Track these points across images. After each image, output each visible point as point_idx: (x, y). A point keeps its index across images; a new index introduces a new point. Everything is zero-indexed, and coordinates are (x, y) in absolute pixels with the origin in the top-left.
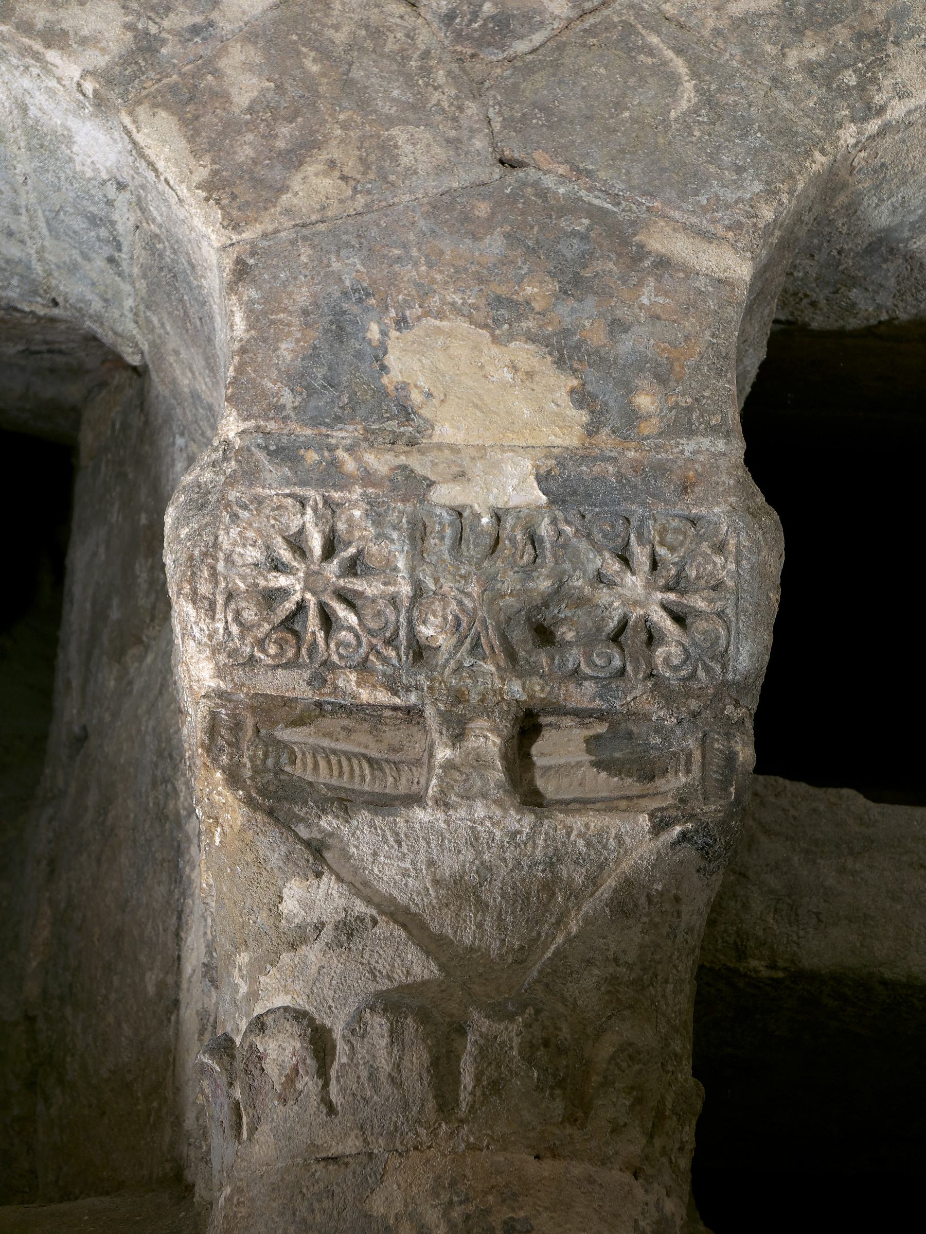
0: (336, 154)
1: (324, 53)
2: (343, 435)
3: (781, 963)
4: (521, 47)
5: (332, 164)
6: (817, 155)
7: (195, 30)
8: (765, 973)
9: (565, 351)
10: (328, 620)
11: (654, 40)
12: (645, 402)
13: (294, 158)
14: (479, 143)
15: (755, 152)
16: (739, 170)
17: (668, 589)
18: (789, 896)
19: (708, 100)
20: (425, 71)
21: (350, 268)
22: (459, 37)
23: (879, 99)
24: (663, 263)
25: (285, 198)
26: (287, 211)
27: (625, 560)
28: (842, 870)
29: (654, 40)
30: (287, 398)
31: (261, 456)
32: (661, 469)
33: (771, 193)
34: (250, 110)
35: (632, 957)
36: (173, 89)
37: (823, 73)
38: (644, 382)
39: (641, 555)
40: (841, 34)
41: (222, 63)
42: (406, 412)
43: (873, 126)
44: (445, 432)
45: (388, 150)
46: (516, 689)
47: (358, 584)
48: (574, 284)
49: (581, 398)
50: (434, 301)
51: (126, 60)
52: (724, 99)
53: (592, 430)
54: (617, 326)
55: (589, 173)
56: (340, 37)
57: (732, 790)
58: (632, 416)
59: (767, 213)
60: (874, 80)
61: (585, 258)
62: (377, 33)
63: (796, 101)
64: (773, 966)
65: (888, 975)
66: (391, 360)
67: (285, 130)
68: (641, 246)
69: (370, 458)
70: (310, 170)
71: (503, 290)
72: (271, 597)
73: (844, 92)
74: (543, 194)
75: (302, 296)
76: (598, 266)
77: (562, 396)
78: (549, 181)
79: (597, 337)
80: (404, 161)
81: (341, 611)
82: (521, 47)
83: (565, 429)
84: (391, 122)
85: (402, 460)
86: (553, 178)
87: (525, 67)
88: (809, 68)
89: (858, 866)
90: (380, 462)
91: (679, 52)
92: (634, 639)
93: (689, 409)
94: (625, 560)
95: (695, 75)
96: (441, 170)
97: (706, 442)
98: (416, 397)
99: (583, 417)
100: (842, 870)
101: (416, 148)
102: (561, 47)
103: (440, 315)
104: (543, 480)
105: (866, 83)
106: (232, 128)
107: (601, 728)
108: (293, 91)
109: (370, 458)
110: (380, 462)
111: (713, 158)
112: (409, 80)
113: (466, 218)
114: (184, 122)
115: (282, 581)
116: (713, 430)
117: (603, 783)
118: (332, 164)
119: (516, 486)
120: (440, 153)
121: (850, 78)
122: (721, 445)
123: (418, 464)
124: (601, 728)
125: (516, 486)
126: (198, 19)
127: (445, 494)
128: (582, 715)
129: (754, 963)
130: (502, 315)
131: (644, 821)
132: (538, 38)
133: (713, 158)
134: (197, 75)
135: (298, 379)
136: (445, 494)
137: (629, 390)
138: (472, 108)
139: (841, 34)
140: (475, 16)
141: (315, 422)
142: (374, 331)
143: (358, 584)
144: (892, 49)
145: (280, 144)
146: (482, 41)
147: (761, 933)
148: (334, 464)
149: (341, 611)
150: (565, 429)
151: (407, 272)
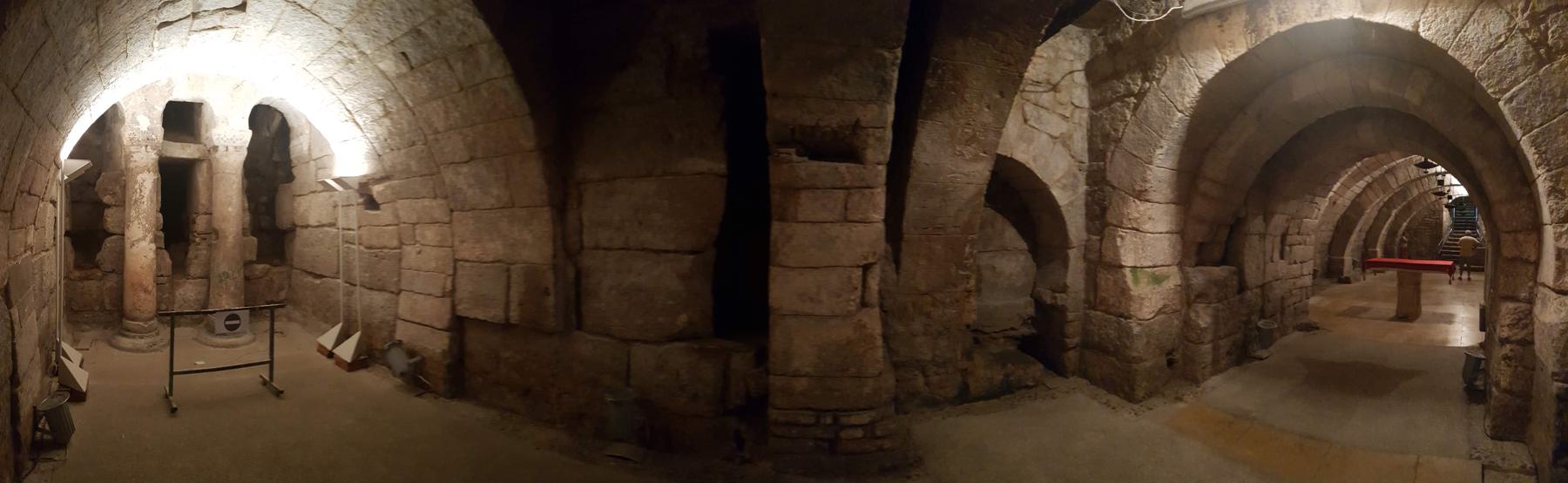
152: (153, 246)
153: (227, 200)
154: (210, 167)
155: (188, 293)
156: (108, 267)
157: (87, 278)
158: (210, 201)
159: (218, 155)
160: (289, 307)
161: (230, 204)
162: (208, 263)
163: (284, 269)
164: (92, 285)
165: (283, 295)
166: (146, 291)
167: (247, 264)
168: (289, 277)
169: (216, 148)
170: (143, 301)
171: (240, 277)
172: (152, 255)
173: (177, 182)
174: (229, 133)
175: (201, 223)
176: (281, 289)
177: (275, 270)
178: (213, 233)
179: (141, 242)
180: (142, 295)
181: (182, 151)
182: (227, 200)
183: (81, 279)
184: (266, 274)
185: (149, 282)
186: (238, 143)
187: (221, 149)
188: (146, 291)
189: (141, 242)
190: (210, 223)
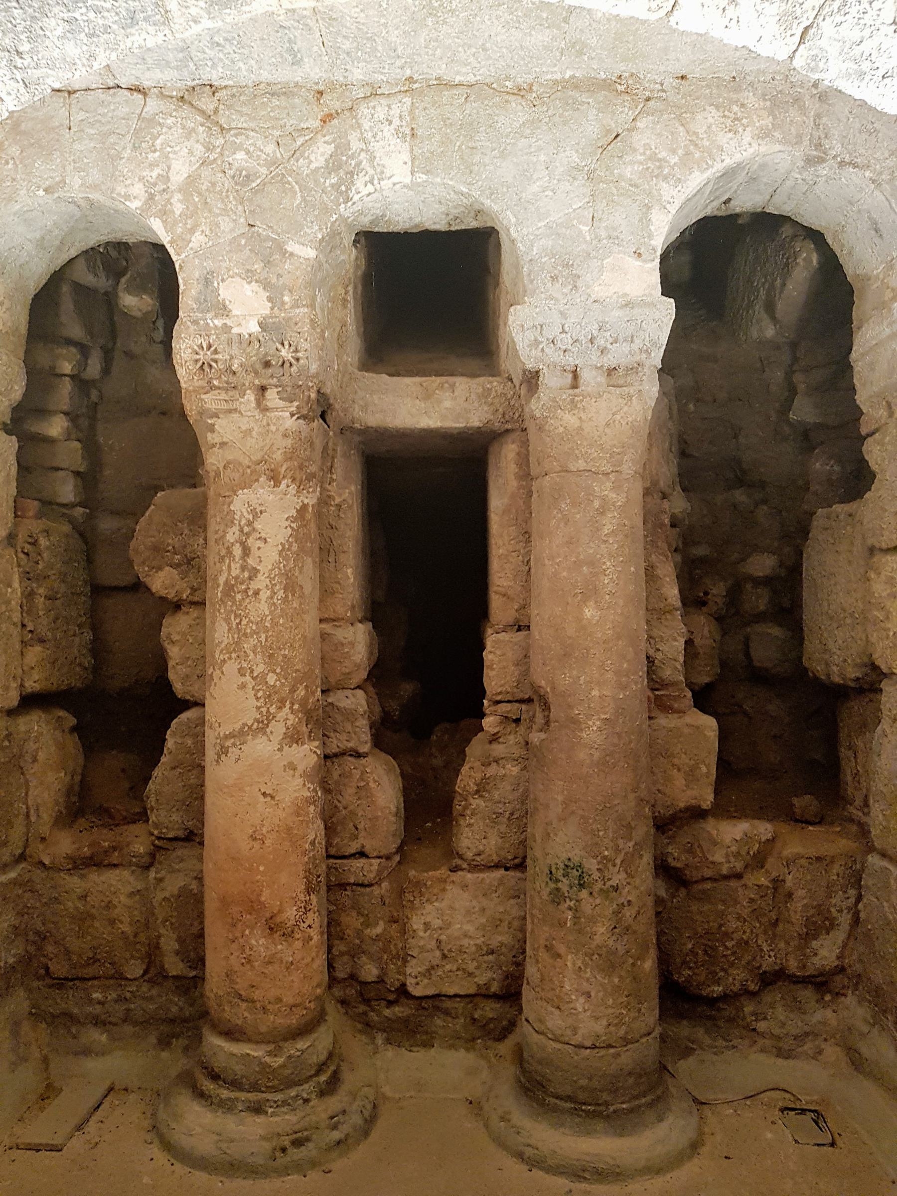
0: (204, 228)
1: (200, 194)
2: (209, 316)
4: (254, 185)
5: (203, 231)
7: (164, 190)
9: (266, 285)
10: (211, 366)
11: (290, 179)
12: (286, 299)
13: (192, 231)
14: (242, 220)
15: (316, 216)
16: (312, 222)
17: (294, 352)
19: (304, 199)
20: (227, 197)
21: (209, 264)
22: (236, 184)
23: (351, 196)
24: (292, 254)
25: (190, 245)
26: (191, 249)
27: (283, 344)
29: (290, 179)
30: (194, 306)
31: (189, 323)
32: (290, 318)
33: (321, 229)
34: (180, 216)
35: (289, 446)
36: (160, 210)
37: (336, 187)
38: (286, 292)
39: (286, 343)
40: (342, 173)
41: (172, 201)
42: (225, 307)
43: (350, 204)
44: (235, 312)
45: (218, 225)
46: (257, 382)
47: (216, 356)
48: (268, 263)
49: (270, 299)
50: (231, 273)
51: (146, 203)
52: (308, 198)
53: (272, 309)
54: (279, 276)
55: (271, 227)
56: (204, 187)
58: (283, 303)
60: (350, 189)
61: (271, 255)
62: (213, 184)
63: (329, 198)
66: (220, 292)
67: (189, 222)
69: (216, 322)
70: (196, 234)
71: (249, 267)
72: (197, 361)
73: (341, 193)
74: (259, 235)
75: (197, 274)
76: (274, 257)
77: (265, 299)
78: (260, 230)
79: (274, 280)
80: (222, 228)
81: (214, 364)
82: (254, 185)
83: (265, 309)
84: (218, 215)
85: (225, 321)
86: (261, 229)
87: (256, 191)
88: (332, 186)
90: (218, 322)
91: (296, 183)
92: (287, 365)
94: (283, 344)
95: (301, 191)
96: (232, 230)
97: (302, 310)
98: (227, 303)
99: (270, 305)
101: (225, 224)
102: (264, 185)
103: (233, 277)
104: (260, 324)
105: (348, 189)
106: (175, 223)
107: (280, 389)
108: (191, 208)
109: (216, 322)
110: (218, 322)
111: (305, 219)
112: (223, 202)
113: (239, 245)
114: (163, 222)
115: (198, 357)
116: (303, 306)
117: (282, 403)
118: (203, 231)
119: (253, 327)
120: (232, 225)
121: (343, 188)
123: (229, 322)
124: (280, 389)
125: (253, 327)
126: (165, 186)
127: (235, 330)
128: (276, 386)
130: (249, 276)
131: (288, 414)
132: (258, 181)
134: (166, 206)
135: (197, 300)
136: (235, 330)
137: (283, 295)
138: (240, 208)
139: (342, 173)
140: (240, 175)
141: (202, 312)
142: (216, 284)
143: (216, 356)
144: (355, 177)
145: (189, 226)
146: (243, 186)
148: (207, 324)
149: (214, 364)
150: (265, 309)
151: (224, 265)
152: (306, 755)
153: (583, 589)
154: (524, 460)
155: (451, 922)
156: (167, 818)
157: (94, 862)
158: (527, 575)
159: (536, 406)
160: (853, 1010)
161: (590, 592)
162: (521, 816)
163: (832, 843)
164: (116, 885)
165: (826, 952)
166: (273, 927)
167: (667, 824)
168: (856, 879)
169: (532, 379)
170: (267, 966)
171: (640, 885)
172: (296, 789)
173: (425, 540)
174: (591, 315)
175: (499, 658)
176: (819, 924)
177: (797, 844)
178: (532, 700)
179: (260, 750)
180: (259, 943)
181: (425, 404)
182: (583, 589)
183: (82, 864)
184: (758, 861)
185: (286, 889)
186: (619, 355)
187: (551, 382)
188: (273, 927)
189: (260, 750)
190: (524, 660)
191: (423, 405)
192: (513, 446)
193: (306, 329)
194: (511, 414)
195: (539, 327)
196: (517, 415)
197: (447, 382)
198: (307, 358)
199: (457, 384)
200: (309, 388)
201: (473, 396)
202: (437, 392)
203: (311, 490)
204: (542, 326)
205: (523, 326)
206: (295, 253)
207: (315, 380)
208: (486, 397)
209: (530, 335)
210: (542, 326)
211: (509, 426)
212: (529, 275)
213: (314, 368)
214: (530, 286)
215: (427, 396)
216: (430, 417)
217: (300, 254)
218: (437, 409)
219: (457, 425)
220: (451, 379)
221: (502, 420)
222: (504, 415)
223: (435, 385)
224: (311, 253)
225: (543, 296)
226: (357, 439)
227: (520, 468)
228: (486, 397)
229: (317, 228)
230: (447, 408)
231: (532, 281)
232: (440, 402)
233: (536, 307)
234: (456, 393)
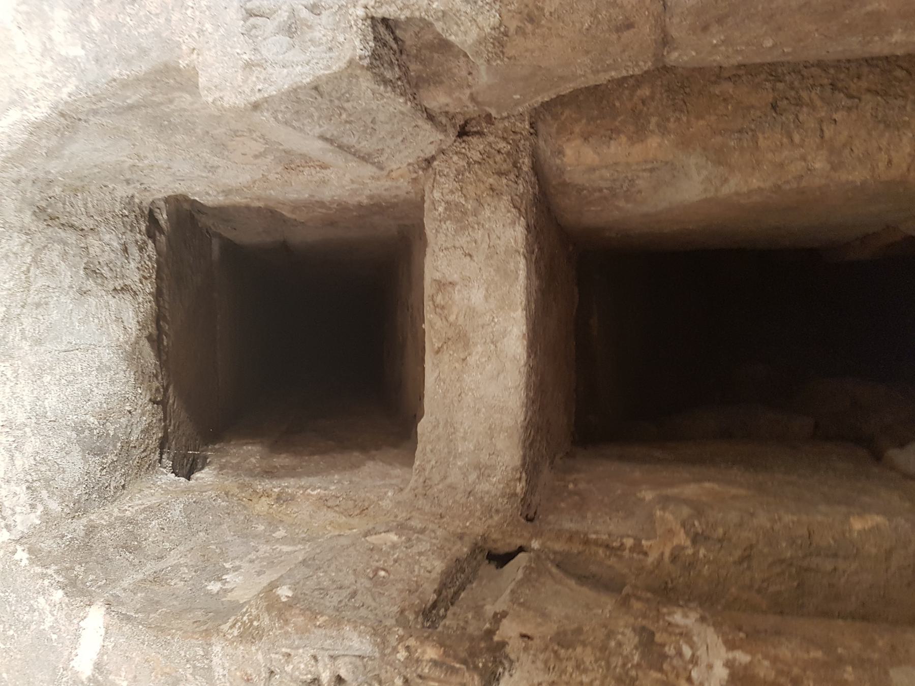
3: (518, 476)
6: (17, 557)
8: (523, 483)
16: (32, 610)
18: (480, 469)
28: (464, 439)
57: (458, 666)
59: (58, 595)
64: (520, 479)
65: (522, 418)
68: (89, 680)
89: (462, 430)
93: (194, 667)
97: (216, 660)
100: (464, 439)
111: (27, 625)
116: (206, 655)
122: (217, 649)
129: (518, 490)
133: (27, 625)
147: (502, 486)
191: (479, 348)
192: (569, 152)
193: (260, 656)
194: (498, 158)
195: (253, 20)
196: (502, 145)
197: (432, 299)
198: (333, 658)
199: (438, 276)
200: (413, 660)
201: (462, 241)
202: (452, 318)
203: (687, 652)
204: (251, 14)
205: (249, 66)
206: (95, 658)
207: (393, 640)
208: (465, 213)
209: (274, 46)
210: (251, 14)
211: (526, 163)
212: (128, 61)
213: (358, 643)
214: (153, 55)
215: (461, 339)
216: (505, 333)
217: (97, 649)
218: (487, 318)
219: (522, 274)
220: (429, 288)
221: (512, 177)
222: (500, 174)
223: (439, 324)
224: (96, 618)
225: (176, 17)
226: (546, 474)
227: (616, 131)
228: (465, 213)
229: (41, 600)
230: (486, 298)
231: (144, 52)
232: (472, 312)
233: (201, 32)
234: (455, 277)
